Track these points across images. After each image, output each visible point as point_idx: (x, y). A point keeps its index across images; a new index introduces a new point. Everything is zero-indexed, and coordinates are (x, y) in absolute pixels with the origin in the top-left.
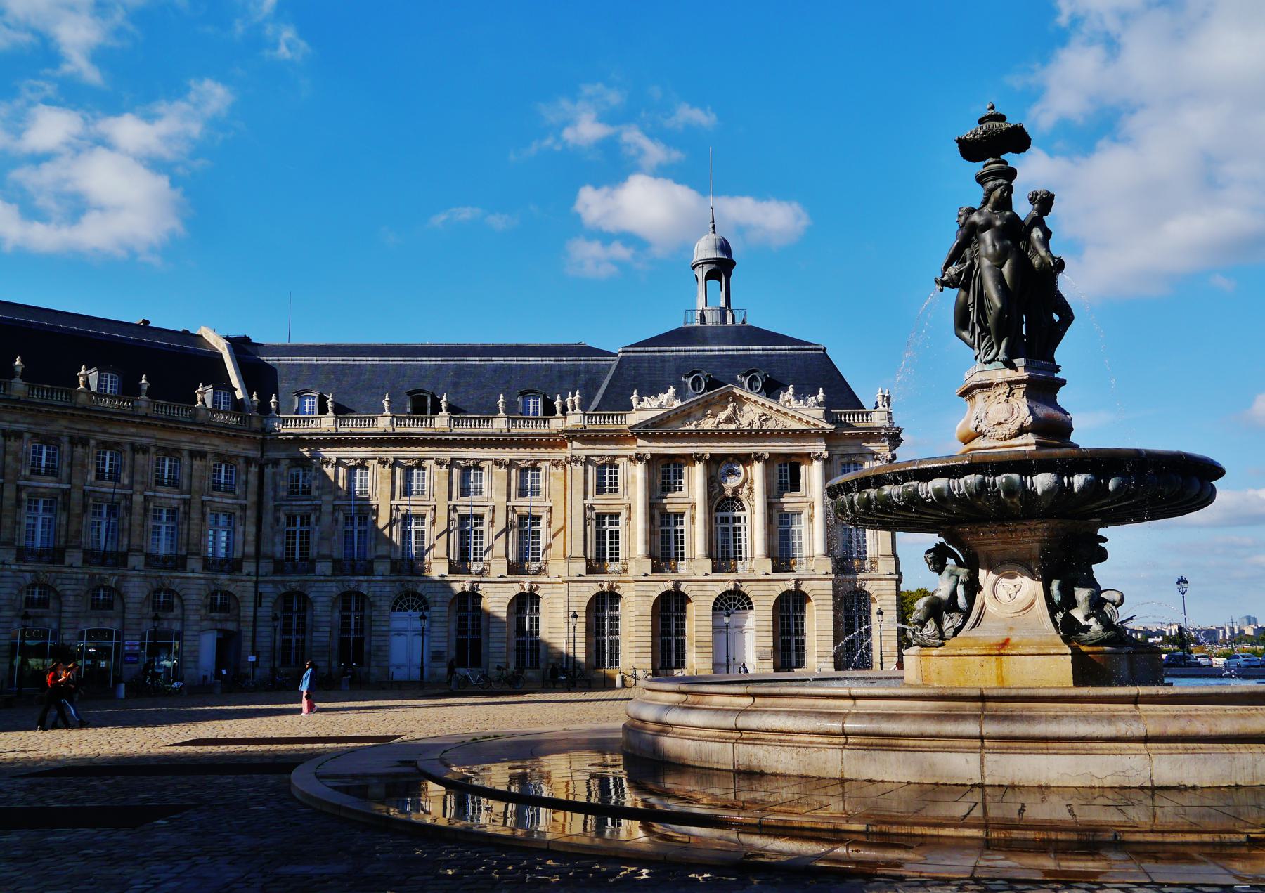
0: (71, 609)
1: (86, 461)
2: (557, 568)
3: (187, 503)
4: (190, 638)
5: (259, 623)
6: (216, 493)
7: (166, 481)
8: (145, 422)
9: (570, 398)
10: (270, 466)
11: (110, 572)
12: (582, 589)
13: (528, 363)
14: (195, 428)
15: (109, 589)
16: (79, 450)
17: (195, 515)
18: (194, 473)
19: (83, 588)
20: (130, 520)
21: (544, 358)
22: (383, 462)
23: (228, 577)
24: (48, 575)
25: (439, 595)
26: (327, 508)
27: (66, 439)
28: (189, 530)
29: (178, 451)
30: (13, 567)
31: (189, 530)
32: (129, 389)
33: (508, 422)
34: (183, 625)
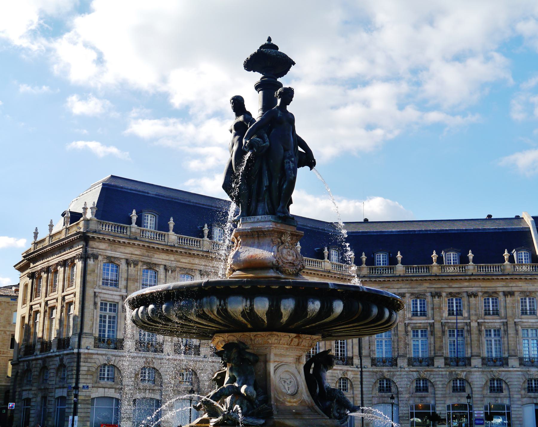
0: (441, 392)
1: (442, 305)
3: (506, 324)
4: (515, 409)
6: (523, 316)
7: (491, 312)
8: (472, 278)
11: (461, 369)
14: (504, 277)
15: (461, 380)
16: (436, 299)
17: (511, 331)
18: (507, 305)
20: (471, 337)
24: (426, 373)
27: (429, 294)
29: (495, 292)
30: (406, 369)
32: (464, 260)
34: (510, 401)
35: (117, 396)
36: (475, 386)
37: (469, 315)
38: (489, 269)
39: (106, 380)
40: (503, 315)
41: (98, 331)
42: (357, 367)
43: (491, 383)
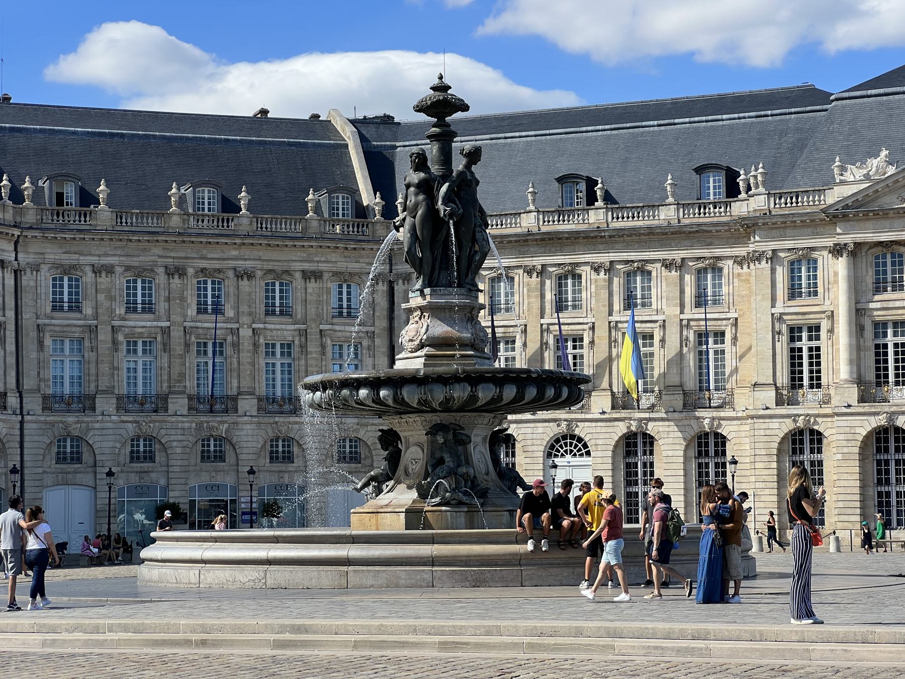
1: (185, 293)
2: (744, 401)
3: (304, 333)
9: (753, 173)
10: (400, 282)
12: (772, 426)
13: (721, 123)
14: (305, 244)
15: (219, 440)
16: (176, 281)
17: (313, 348)
18: (309, 297)
19: (190, 438)
21: (742, 115)
22: (529, 271)
23: (356, 420)
24: (152, 425)
25: (602, 436)
27: (161, 270)
28: (307, 366)
29: (287, 272)
31: (307, 366)
33: (678, 209)
36: (245, 451)
37: (238, 314)
38: (279, 226)
40: (299, 316)
42: (14, 413)
43: (272, 446)
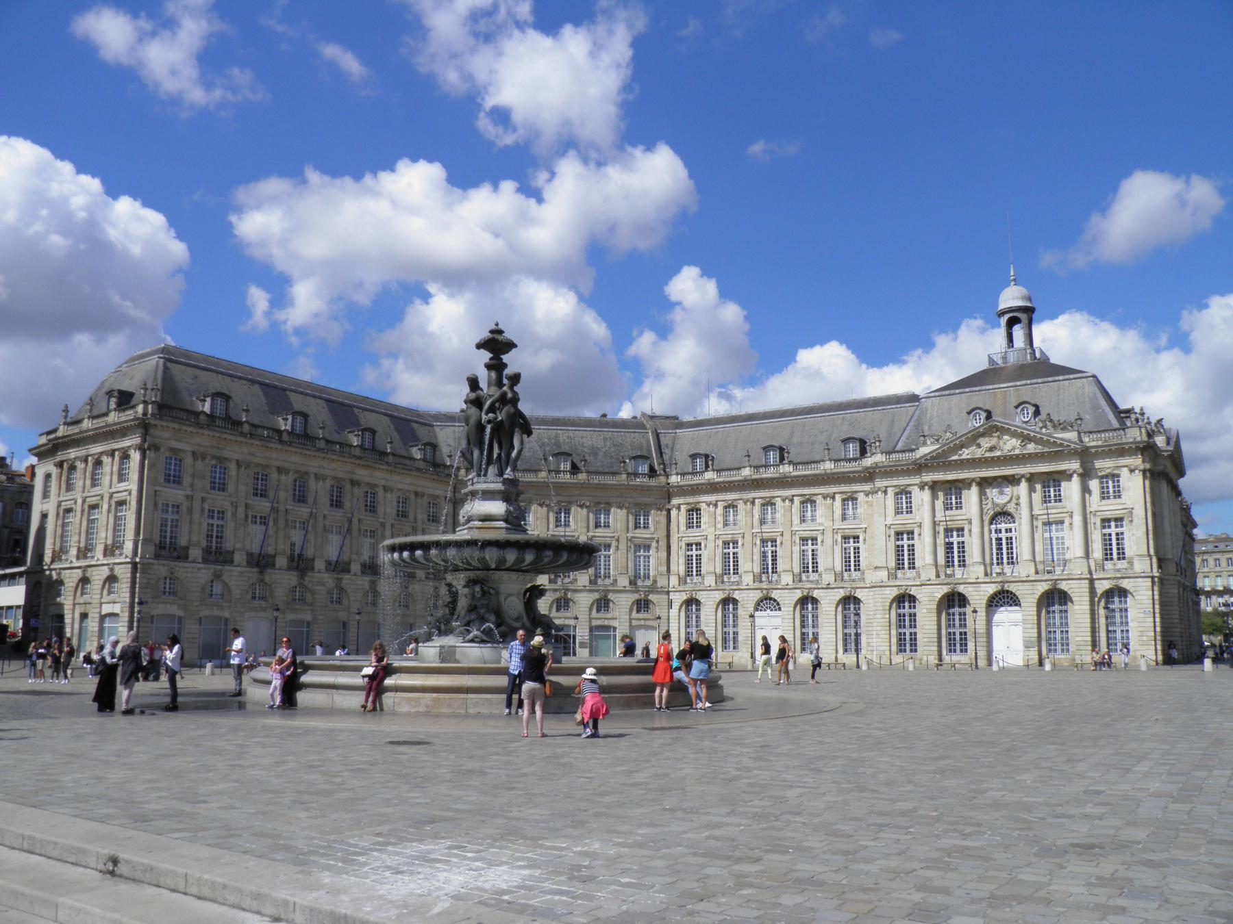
2: (872, 577)
5: (671, 621)
12: (886, 592)
25: (787, 598)
26: (711, 537)
35: (180, 613)
39: (167, 594)
41: (158, 536)
